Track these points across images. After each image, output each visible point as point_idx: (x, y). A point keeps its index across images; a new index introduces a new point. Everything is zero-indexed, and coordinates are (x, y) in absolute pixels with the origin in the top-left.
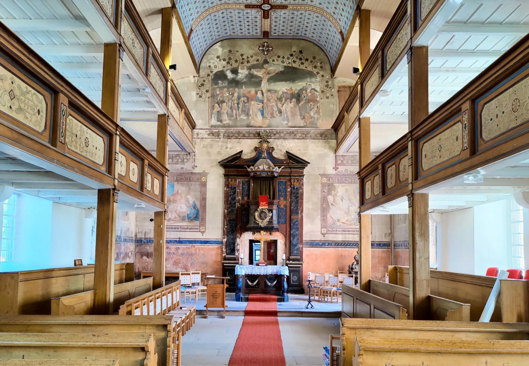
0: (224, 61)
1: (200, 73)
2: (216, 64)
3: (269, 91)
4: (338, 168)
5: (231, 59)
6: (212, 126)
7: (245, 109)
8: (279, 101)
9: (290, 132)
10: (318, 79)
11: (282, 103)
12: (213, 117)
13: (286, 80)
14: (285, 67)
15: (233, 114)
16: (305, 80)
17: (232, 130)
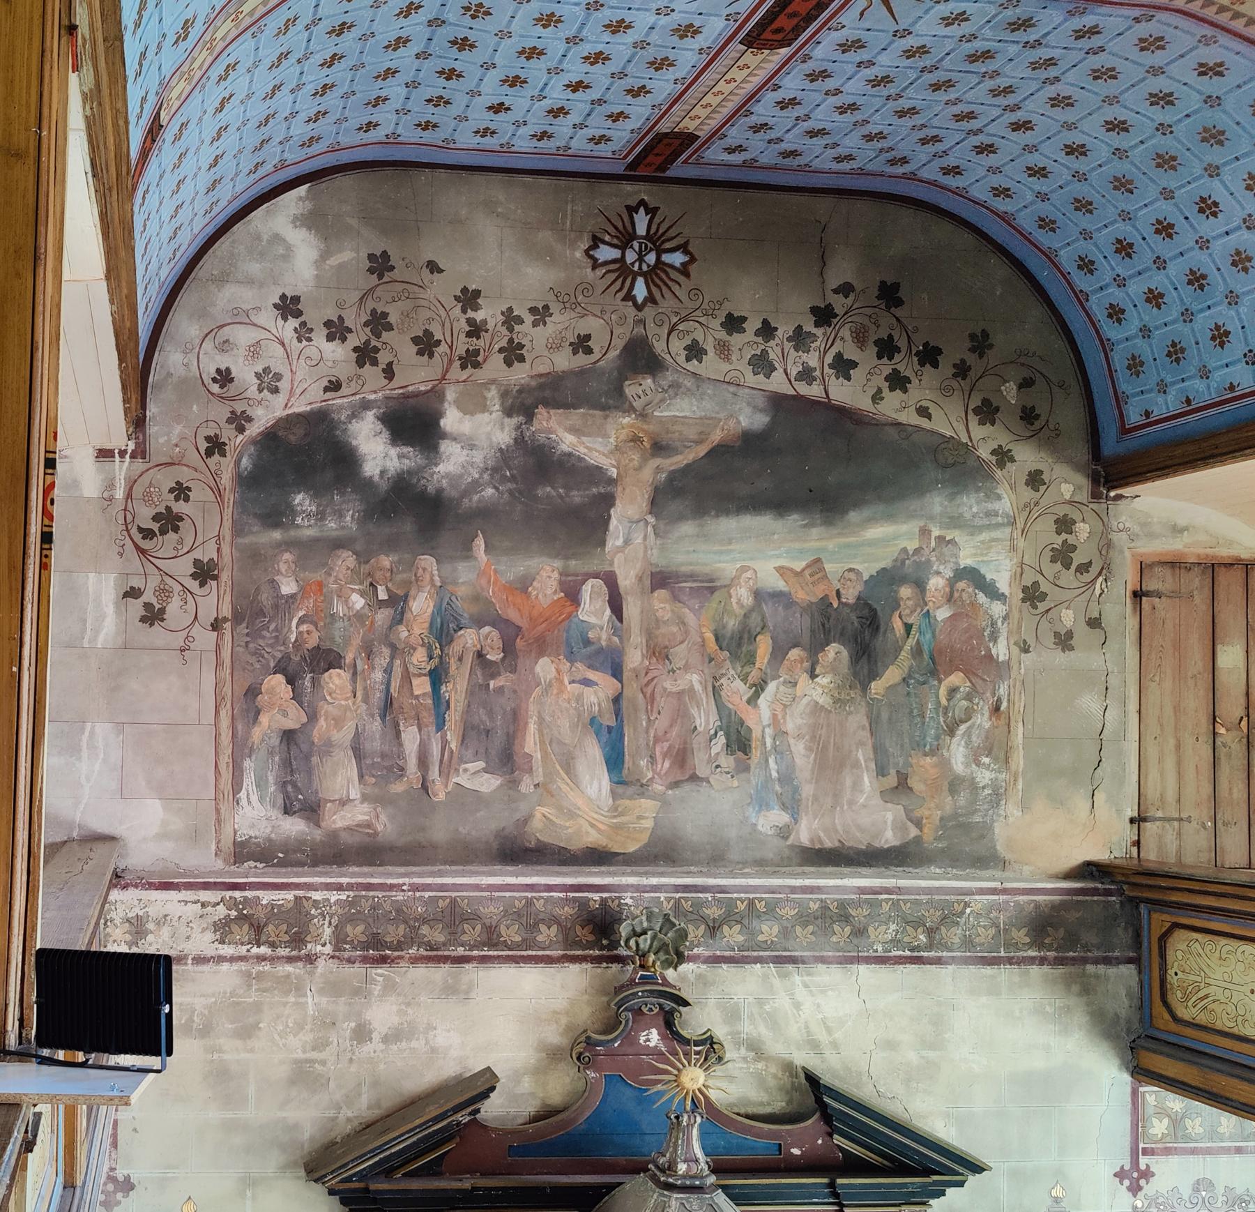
0: (330, 338)
1: (152, 429)
2: (274, 357)
3: (661, 580)
4: (1147, 1174)
5: (389, 327)
6: (242, 852)
7: (491, 713)
8: (735, 657)
9: (825, 907)
10: (1006, 503)
11: (754, 675)
12: (249, 781)
13: (779, 504)
14: (778, 402)
15: (401, 755)
16: (914, 504)
17: (400, 897)
